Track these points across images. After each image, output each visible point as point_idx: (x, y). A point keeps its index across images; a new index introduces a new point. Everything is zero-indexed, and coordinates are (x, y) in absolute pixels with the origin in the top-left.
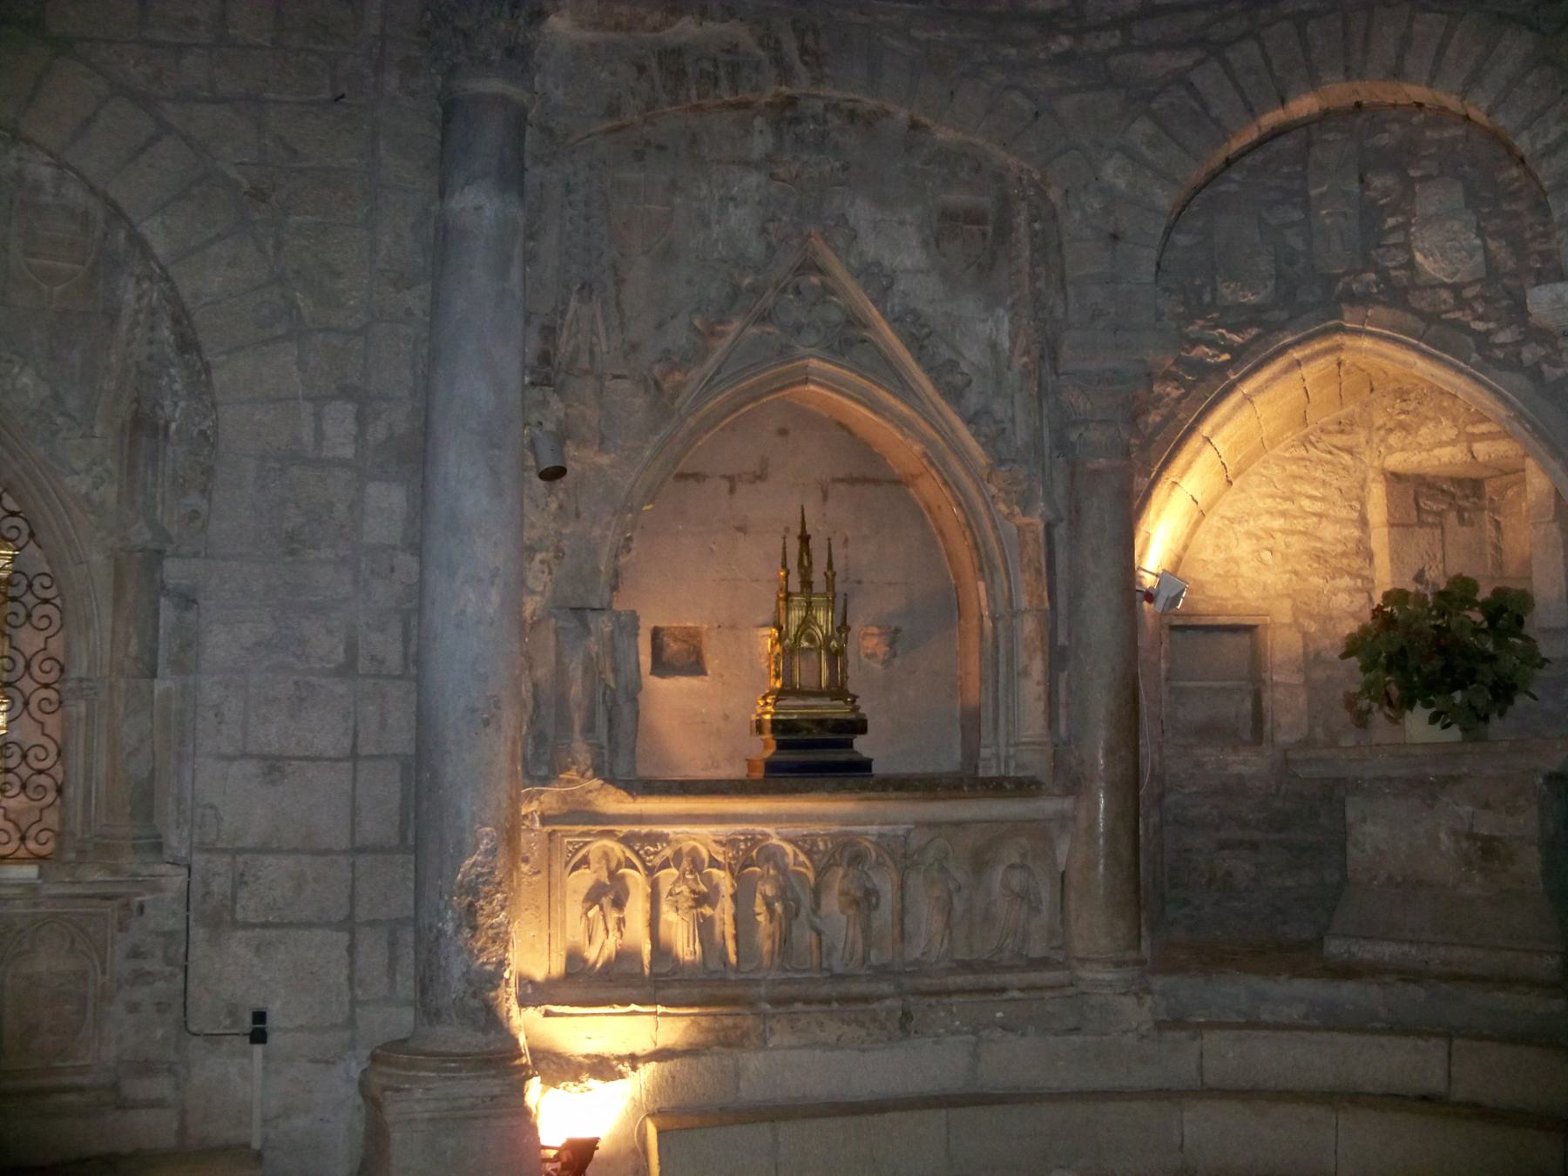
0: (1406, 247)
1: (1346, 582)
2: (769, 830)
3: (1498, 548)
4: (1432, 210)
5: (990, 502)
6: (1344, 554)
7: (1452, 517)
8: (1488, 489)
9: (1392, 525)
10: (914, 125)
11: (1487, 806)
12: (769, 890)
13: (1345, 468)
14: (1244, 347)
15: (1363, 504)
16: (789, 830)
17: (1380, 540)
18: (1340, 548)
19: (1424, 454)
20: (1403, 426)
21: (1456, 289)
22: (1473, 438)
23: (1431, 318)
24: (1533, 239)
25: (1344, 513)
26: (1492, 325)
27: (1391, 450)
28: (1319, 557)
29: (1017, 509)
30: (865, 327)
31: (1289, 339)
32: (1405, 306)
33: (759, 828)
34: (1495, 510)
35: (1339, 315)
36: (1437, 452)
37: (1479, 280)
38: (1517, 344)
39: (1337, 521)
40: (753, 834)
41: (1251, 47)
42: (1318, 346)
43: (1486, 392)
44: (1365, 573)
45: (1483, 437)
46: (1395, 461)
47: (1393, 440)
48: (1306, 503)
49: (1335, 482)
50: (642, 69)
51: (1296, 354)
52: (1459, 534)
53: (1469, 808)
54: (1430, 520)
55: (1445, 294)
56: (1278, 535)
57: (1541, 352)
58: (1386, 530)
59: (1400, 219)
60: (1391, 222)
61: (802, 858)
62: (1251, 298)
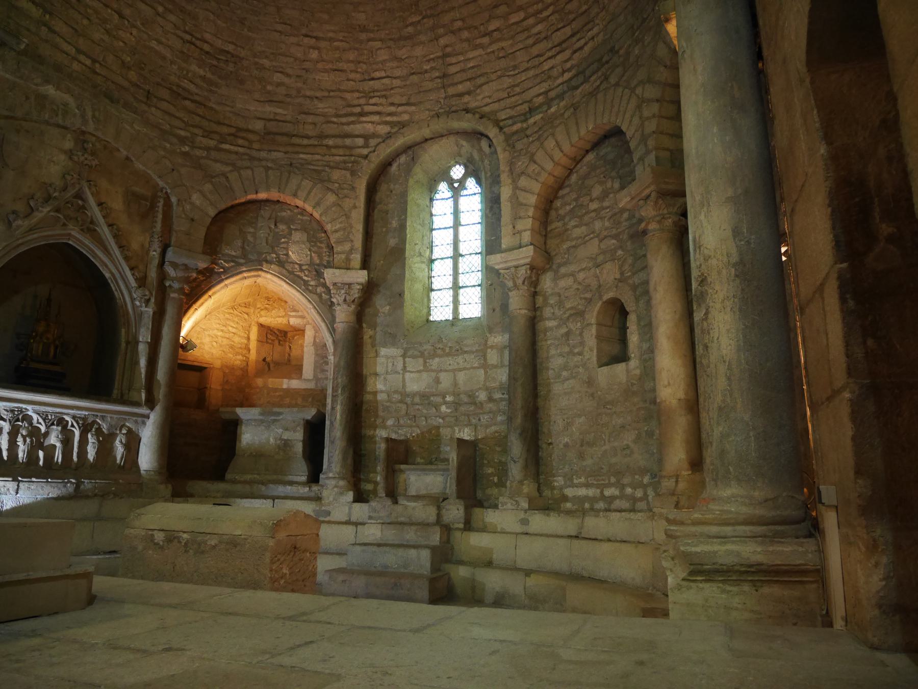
0: (287, 249)
1: (240, 357)
2: (29, 407)
3: (289, 355)
4: (297, 239)
6: (241, 348)
7: (276, 342)
8: (289, 335)
9: (258, 341)
10: (127, 158)
11: (287, 429)
12: (24, 433)
13: (245, 319)
14: (229, 268)
15: (249, 332)
16: (37, 408)
17: (253, 345)
18: (239, 346)
19: (273, 319)
20: (266, 309)
21: (300, 265)
24: (325, 256)
25: (243, 334)
26: (309, 279)
27: (261, 316)
28: (232, 347)
29: (144, 305)
30: (97, 226)
31: (245, 269)
32: (283, 267)
33: (24, 406)
34: (290, 343)
36: (277, 319)
37: (307, 264)
38: (316, 286)
39: (240, 336)
40: (22, 408)
41: (249, 172)
42: (252, 273)
43: (305, 298)
44: (247, 355)
45: (293, 316)
46: (262, 320)
47: (263, 313)
48: (230, 328)
49: (241, 324)
50: (27, 98)
51: (245, 275)
52: (278, 348)
53: (281, 430)
54: (270, 341)
55: (297, 266)
56: (219, 337)
57: (323, 290)
58: (256, 342)
59: (286, 240)
60: (283, 240)
61: (41, 421)
62: (234, 253)
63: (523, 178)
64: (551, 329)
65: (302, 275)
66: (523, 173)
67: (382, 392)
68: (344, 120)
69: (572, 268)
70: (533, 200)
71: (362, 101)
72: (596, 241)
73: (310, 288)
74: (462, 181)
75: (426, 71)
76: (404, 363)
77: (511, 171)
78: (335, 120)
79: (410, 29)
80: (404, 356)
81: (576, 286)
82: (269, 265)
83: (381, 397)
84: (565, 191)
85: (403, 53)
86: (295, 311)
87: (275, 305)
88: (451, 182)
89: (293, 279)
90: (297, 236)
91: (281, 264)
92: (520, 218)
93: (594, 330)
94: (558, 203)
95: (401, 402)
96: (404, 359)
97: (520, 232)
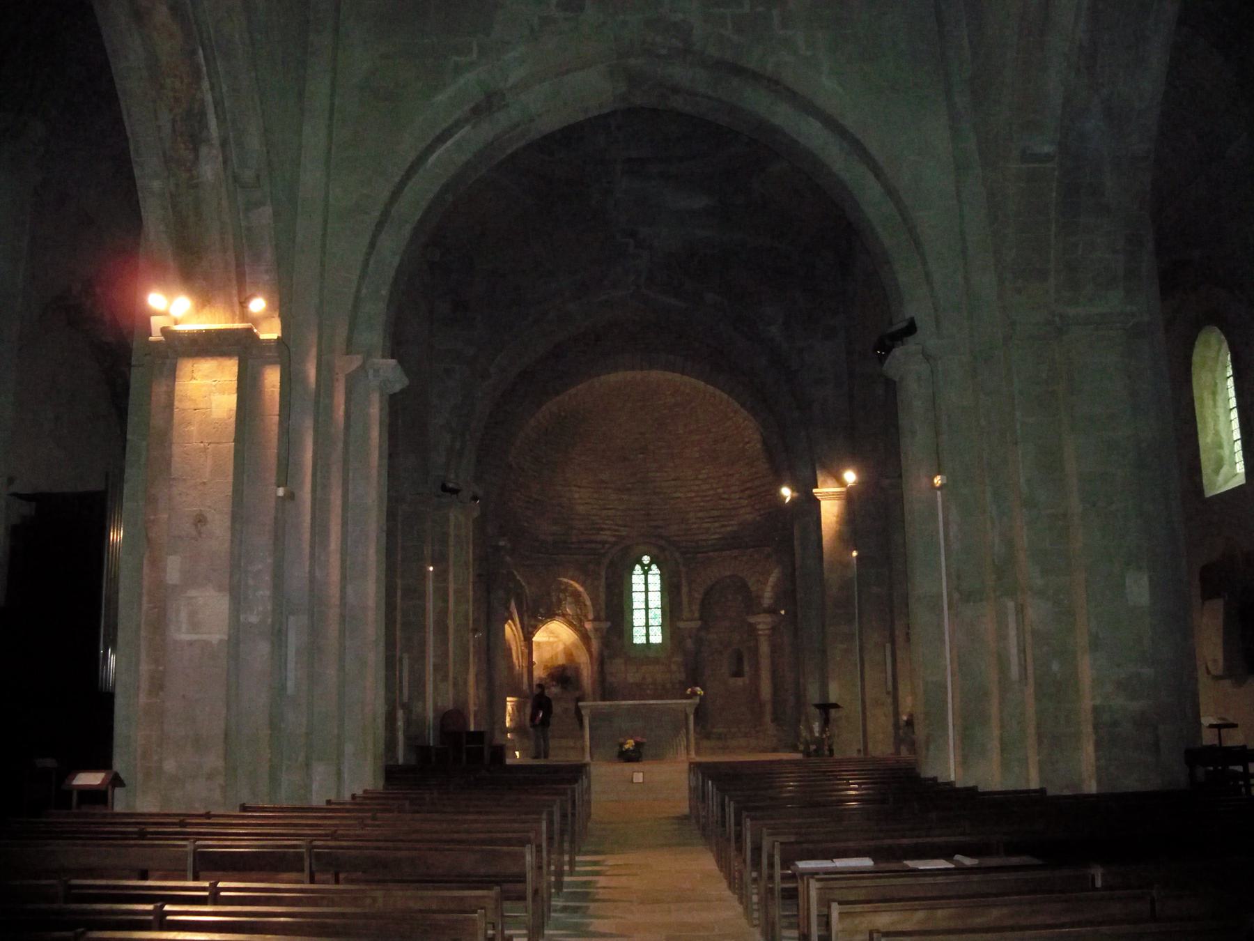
0: (565, 607)
5: (521, 646)
23: (568, 621)
68: (591, 532)
71: (601, 521)
74: (649, 565)
75: (637, 510)
78: (586, 532)
79: (630, 486)
85: (625, 497)
86: (553, 633)
88: (643, 566)
89: (570, 624)
91: (564, 615)
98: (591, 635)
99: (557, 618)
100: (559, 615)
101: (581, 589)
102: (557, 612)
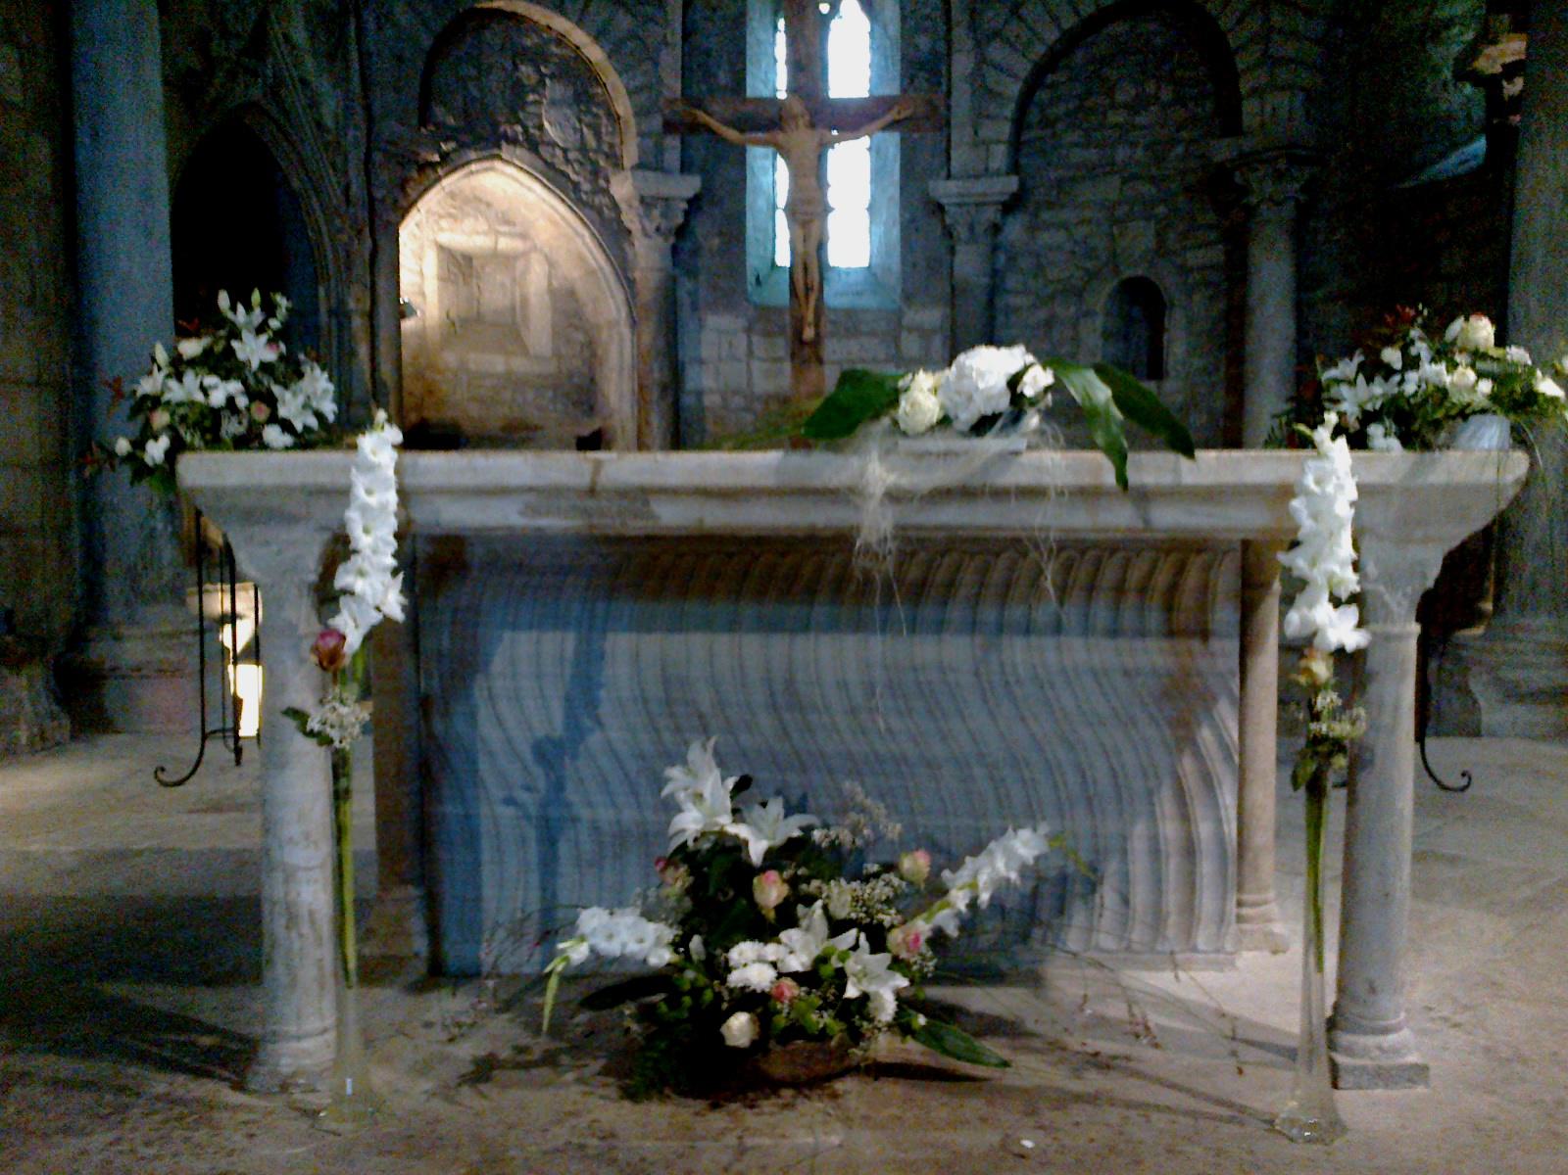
0: (539, 116)
20: (450, 215)
22: (498, 233)
23: (550, 166)
27: (441, 229)
34: (478, 278)
35: (499, 147)
45: (504, 234)
47: (444, 223)
55: (559, 152)
59: (537, 97)
63: (996, 44)
64: (1017, 309)
65: (569, 170)
66: (997, 34)
67: (712, 391)
69: (1067, 215)
70: (1014, 89)
72: (1116, 180)
73: (584, 197)
76: (750, 344)
77: (973, 27)
80: (749, 331)
81: (1068, 246)
82: (511, 148)
83: (711, 400)
84: (1060, 77)
86: (507, 222)
87: (467, 209)
89: (554, 177)
90: (554, 90)
91: (533, 145)
92: (988, 117)
93: (1099, 322)
94: (1042, 95)
95: (747, 409)
96: (749, 337)
97: (986, 144)
98: (630, 219)
99: (506, 151)
100: (513, 141)
101: (595, 53)
102: (505, 128)
